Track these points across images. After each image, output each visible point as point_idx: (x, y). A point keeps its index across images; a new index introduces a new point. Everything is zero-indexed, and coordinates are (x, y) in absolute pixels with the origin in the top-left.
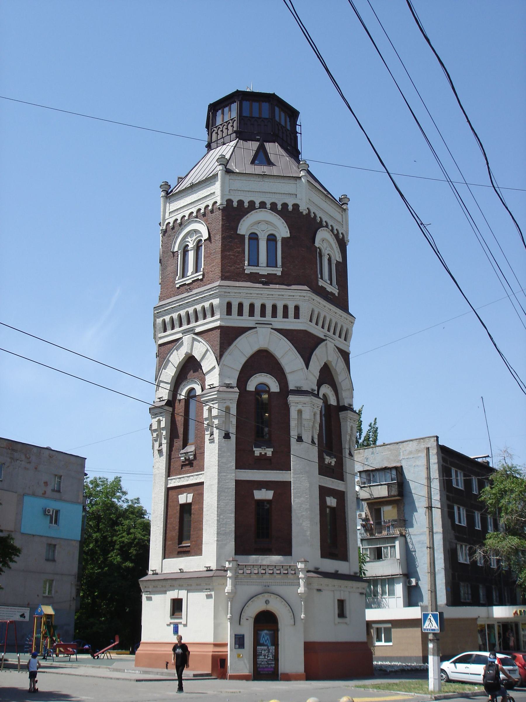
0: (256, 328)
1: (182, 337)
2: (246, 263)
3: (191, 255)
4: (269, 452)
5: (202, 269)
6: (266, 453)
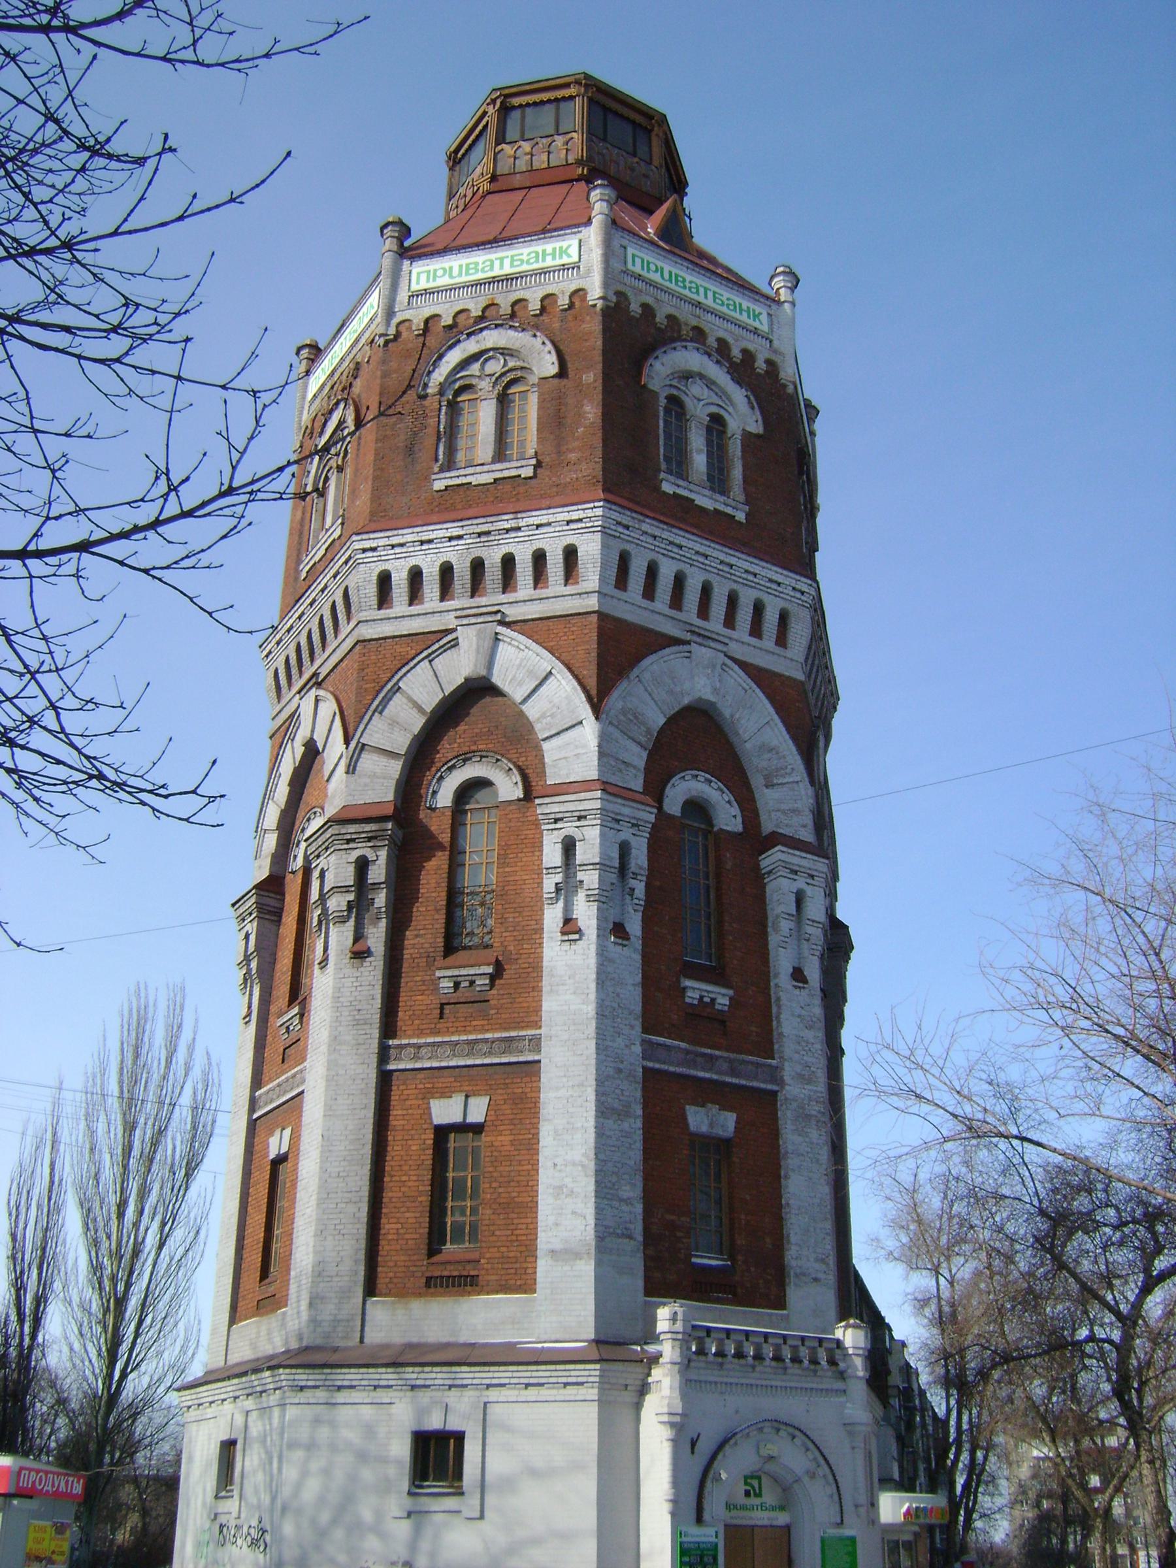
0: (688, 643)
1: (454, 630)
4: (722, 997)
6: (713, 1000)
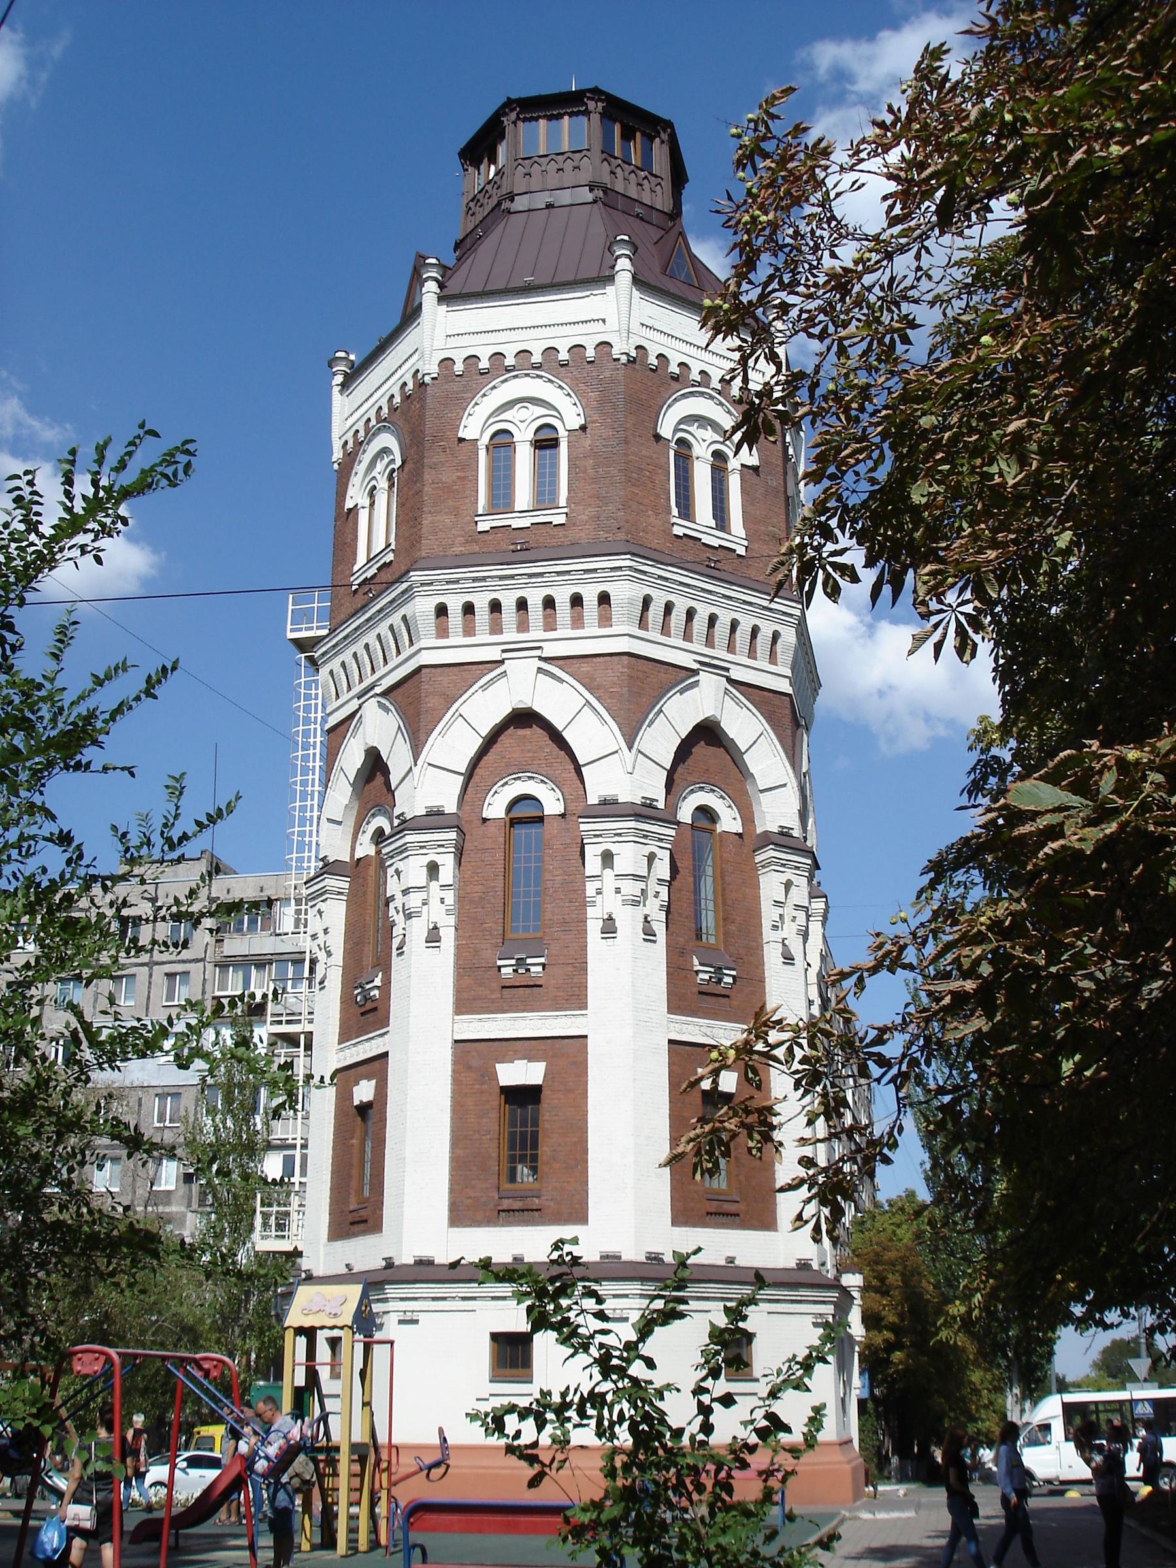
2: (675, 512)
3: (524, 458)
5: (562, 502)
